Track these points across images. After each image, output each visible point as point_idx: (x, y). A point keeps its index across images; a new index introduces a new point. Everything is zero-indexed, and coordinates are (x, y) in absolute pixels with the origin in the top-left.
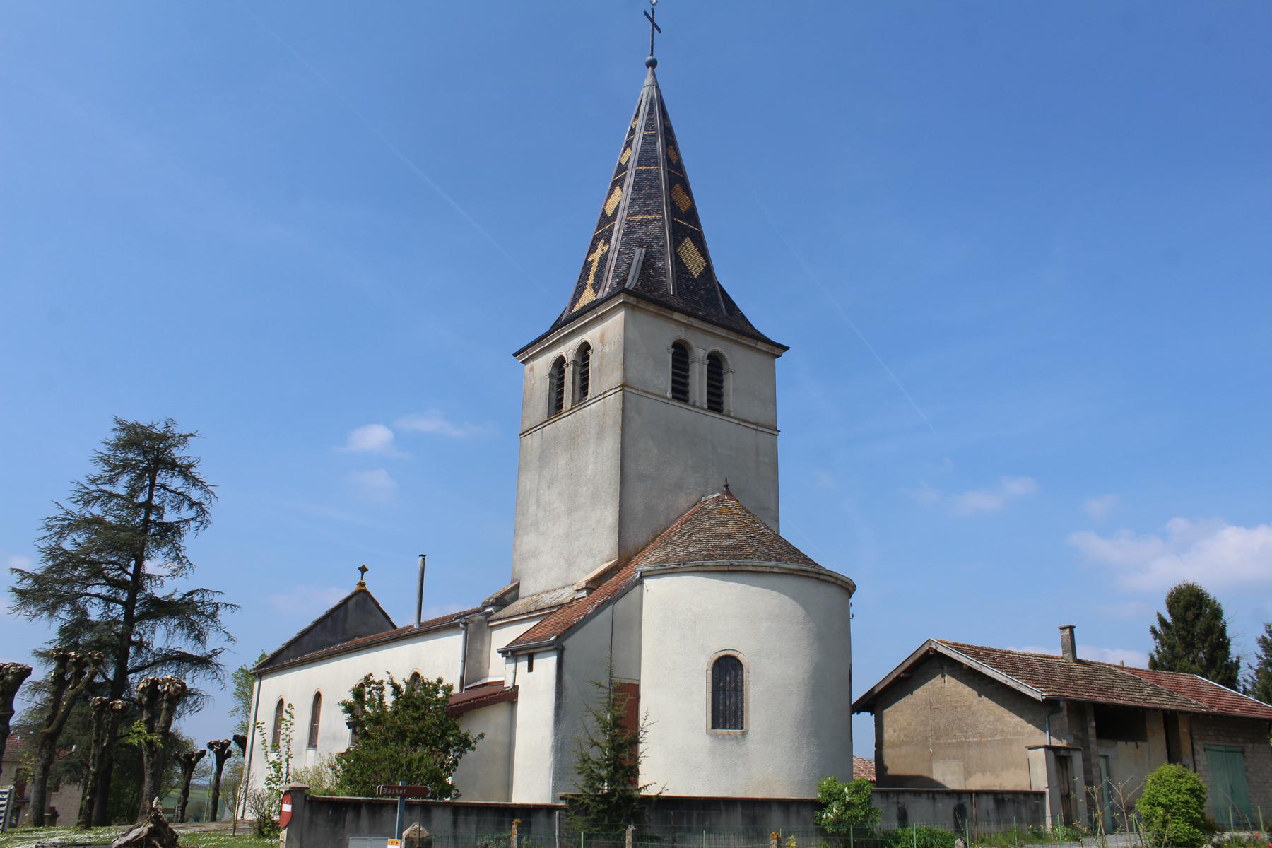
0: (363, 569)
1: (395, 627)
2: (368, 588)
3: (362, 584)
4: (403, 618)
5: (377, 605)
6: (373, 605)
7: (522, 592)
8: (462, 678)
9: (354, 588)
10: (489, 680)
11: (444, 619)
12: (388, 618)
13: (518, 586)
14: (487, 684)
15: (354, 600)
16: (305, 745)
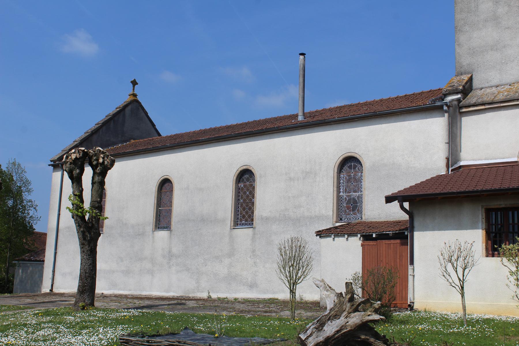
0: (134, 83)
1: (159, 135)
2: (139, 98)
3: (135, 95)
4: (167, 128)
5: (146, 113)
6: (143, 114)
7: (476, 84)
8: (448, 159)
9: (126, 98)
10: (462, 163)
11: (212, 130)
12: (153, 125)
13: (471, 79)
14: (460, 167)
15: (129, 108)
16: (150, 227)
